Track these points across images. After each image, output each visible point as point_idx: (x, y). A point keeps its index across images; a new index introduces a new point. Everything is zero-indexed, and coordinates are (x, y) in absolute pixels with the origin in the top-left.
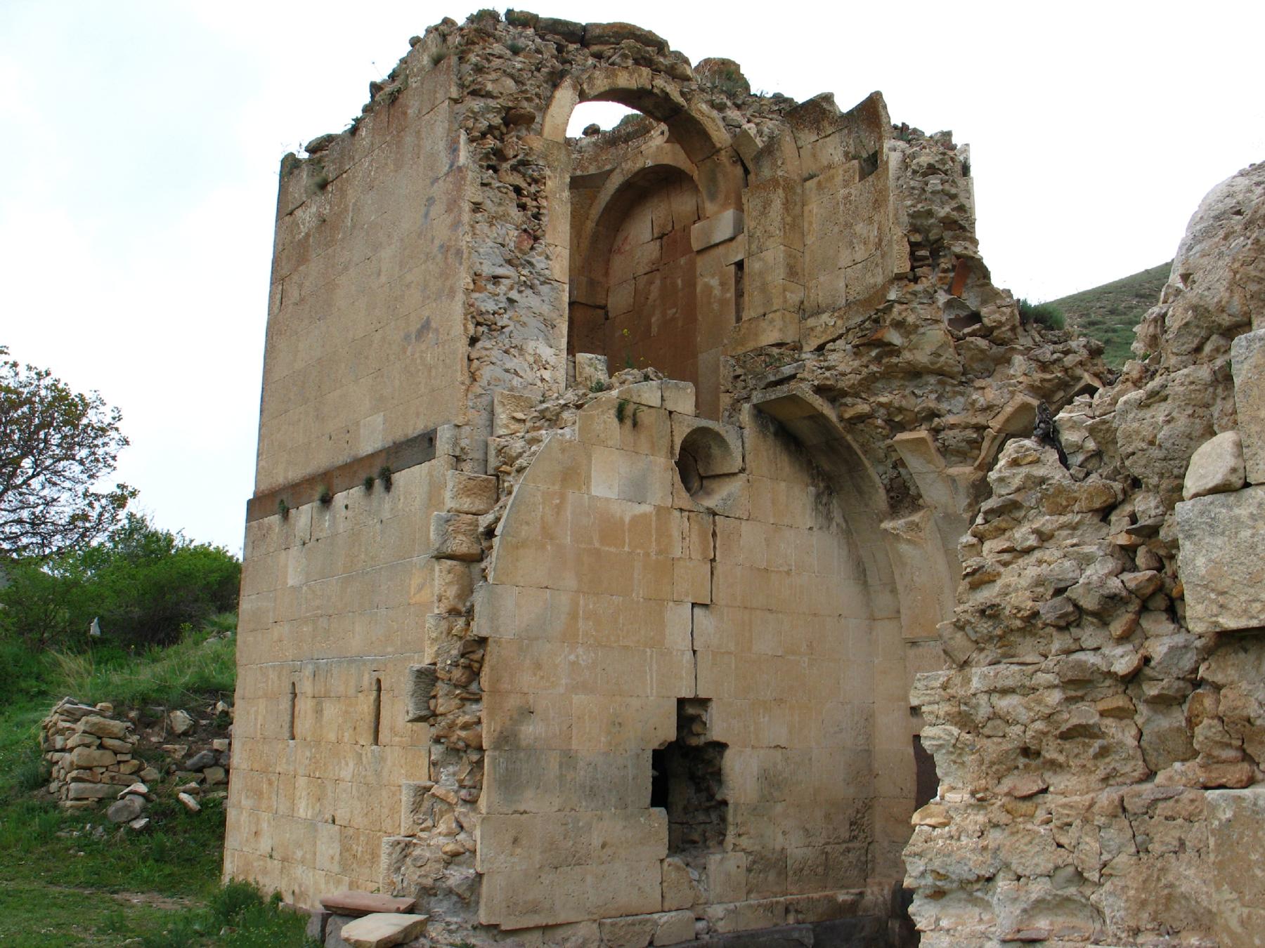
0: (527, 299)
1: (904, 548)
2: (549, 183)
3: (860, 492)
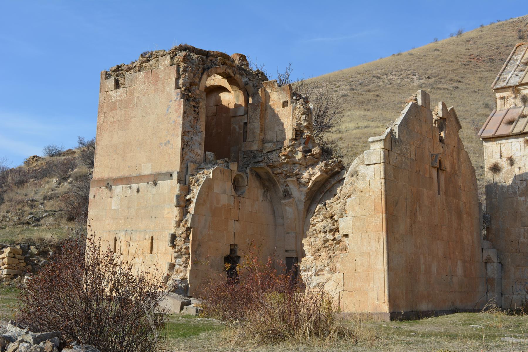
0: (195, 138)
1: (287, 208)
2: (201, 104)
3: (276, 192)
